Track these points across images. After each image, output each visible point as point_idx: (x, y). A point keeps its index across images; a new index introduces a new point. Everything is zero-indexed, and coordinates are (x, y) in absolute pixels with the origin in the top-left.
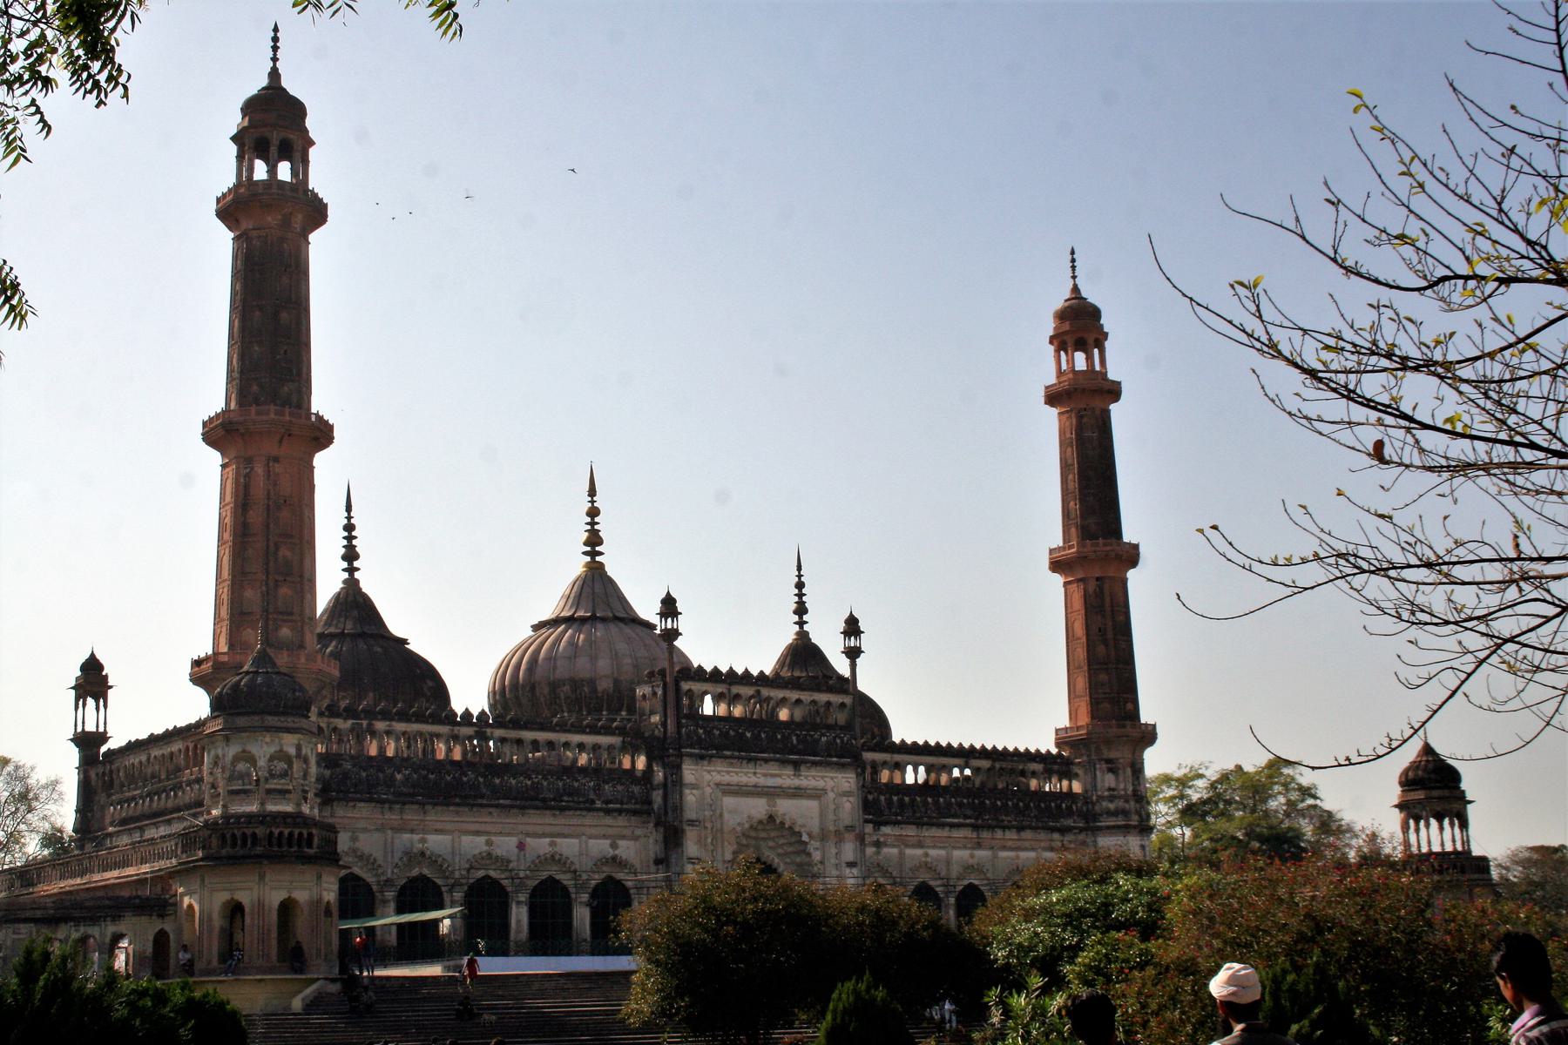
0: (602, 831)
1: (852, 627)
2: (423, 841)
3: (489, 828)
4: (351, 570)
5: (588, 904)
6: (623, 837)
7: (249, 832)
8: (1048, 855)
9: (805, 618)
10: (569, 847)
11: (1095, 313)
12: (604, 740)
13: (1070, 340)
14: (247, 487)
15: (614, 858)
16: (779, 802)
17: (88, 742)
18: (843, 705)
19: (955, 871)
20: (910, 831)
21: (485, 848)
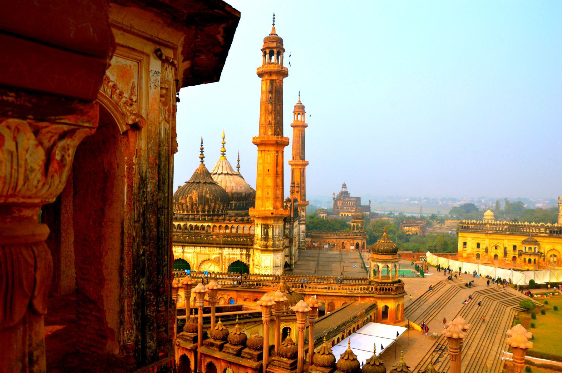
4: (202, 162)
11: (303, 107)
14: (277, 160)
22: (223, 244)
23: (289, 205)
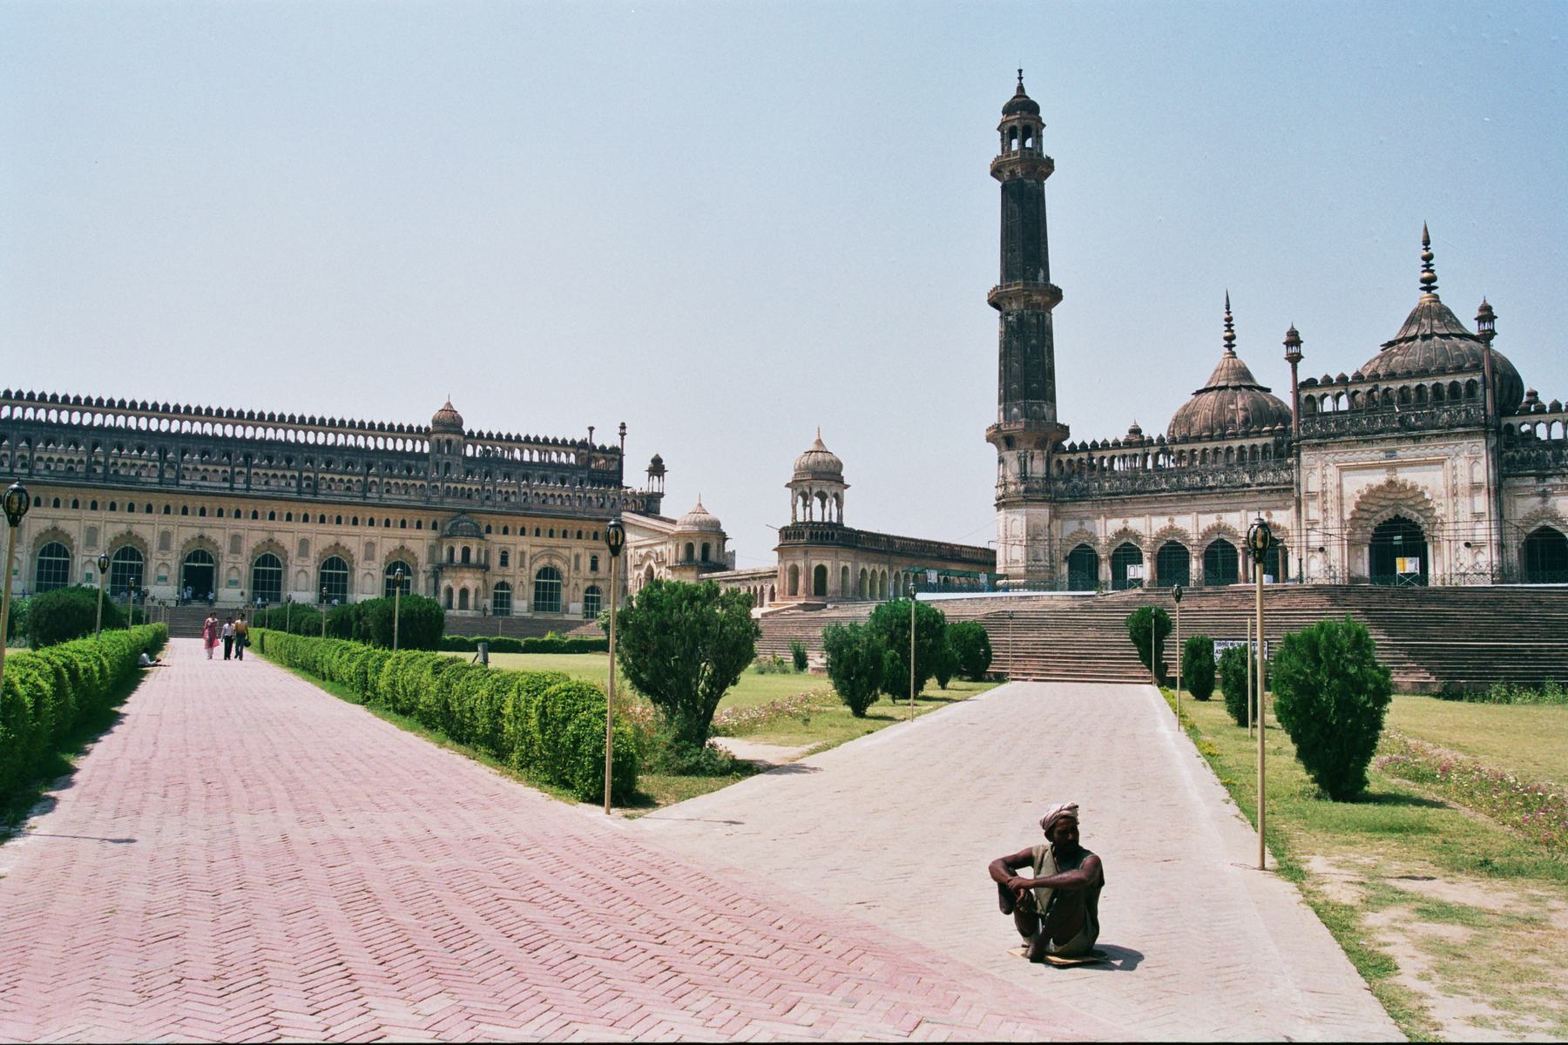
1: (1487, 315)
4: (1230, 346)
6: (1277, 508)
12: (1259, 442)
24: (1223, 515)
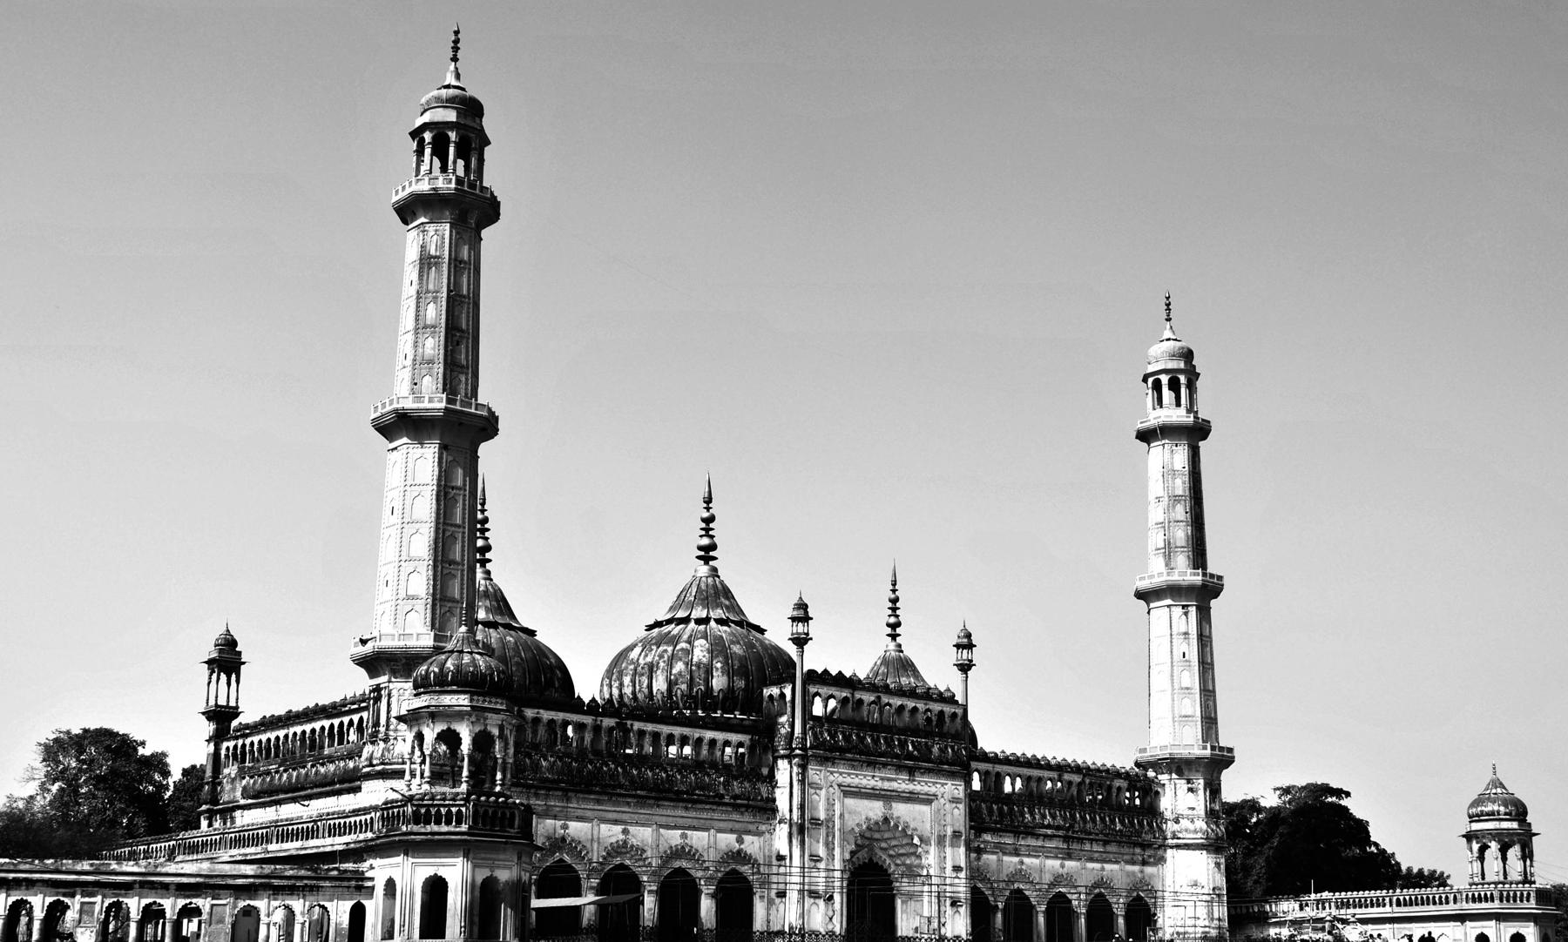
0: (730, 825)
2: (565, 827)
3: (625, 817)
5: (713, 896)
6: (749, 832)
7: (454, 810)
8: (1130, 868)
9: (898, 630)
10: (699, 839)
13: (1165, 379)
15: (739, 852)
16: (894, 805)
17: (221, 717)
18: (954, 715)
19: (1047, 878)
20: (1008, 840)
21: (622, 837)
22: (341, 782)
23: (788, 691)
24: (689, 832)
